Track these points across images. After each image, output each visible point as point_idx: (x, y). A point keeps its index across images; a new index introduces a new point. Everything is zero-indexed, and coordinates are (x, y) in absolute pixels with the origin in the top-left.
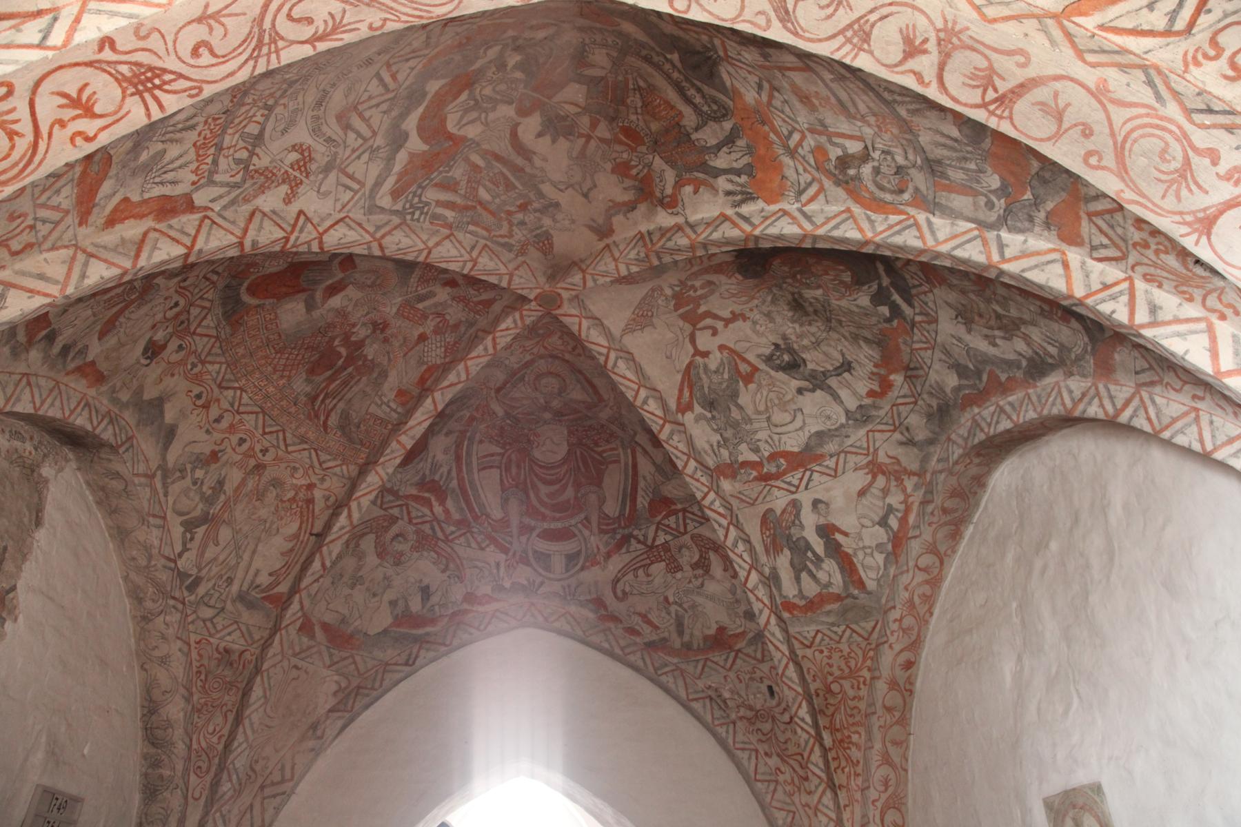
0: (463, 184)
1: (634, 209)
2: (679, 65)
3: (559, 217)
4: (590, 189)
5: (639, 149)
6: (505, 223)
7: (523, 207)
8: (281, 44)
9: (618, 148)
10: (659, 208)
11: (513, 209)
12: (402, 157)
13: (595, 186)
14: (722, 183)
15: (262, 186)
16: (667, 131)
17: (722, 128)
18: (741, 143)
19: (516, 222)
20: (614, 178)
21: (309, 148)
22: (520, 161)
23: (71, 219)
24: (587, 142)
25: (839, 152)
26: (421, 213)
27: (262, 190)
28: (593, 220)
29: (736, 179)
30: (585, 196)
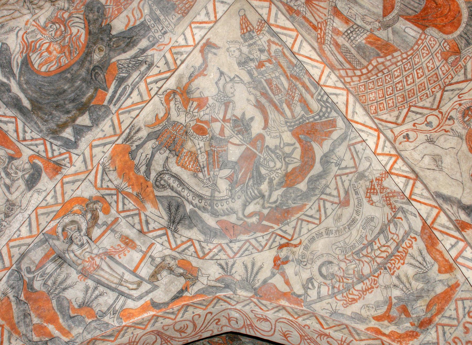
0: (296, 98)
1: (191, 76)
2: (186, 203)
3: (237, 53)
4: (219, 80)
5: (195, 122)
6: (273, 54)
7: (261, 64)
8: (340, 342)
9: (207, 118)
10: (175, 88)
11: (267, 64)
12: (327, 145)
13: (216, 83)
14: (144, 133)
15: (394, 196)
16: (182, 146)
17: (154, 170)
18: (143, 169)
19: (266, 53)
20: (206, 94)
21: (366, 197)
22: (263, 100)
23: (459, 294)
24: (224, 117)
25: (100, 222)
26: (322, 96)
27: (394, 194)
28: (215, 54)
29: (137, 143)
30: (222, 73)
